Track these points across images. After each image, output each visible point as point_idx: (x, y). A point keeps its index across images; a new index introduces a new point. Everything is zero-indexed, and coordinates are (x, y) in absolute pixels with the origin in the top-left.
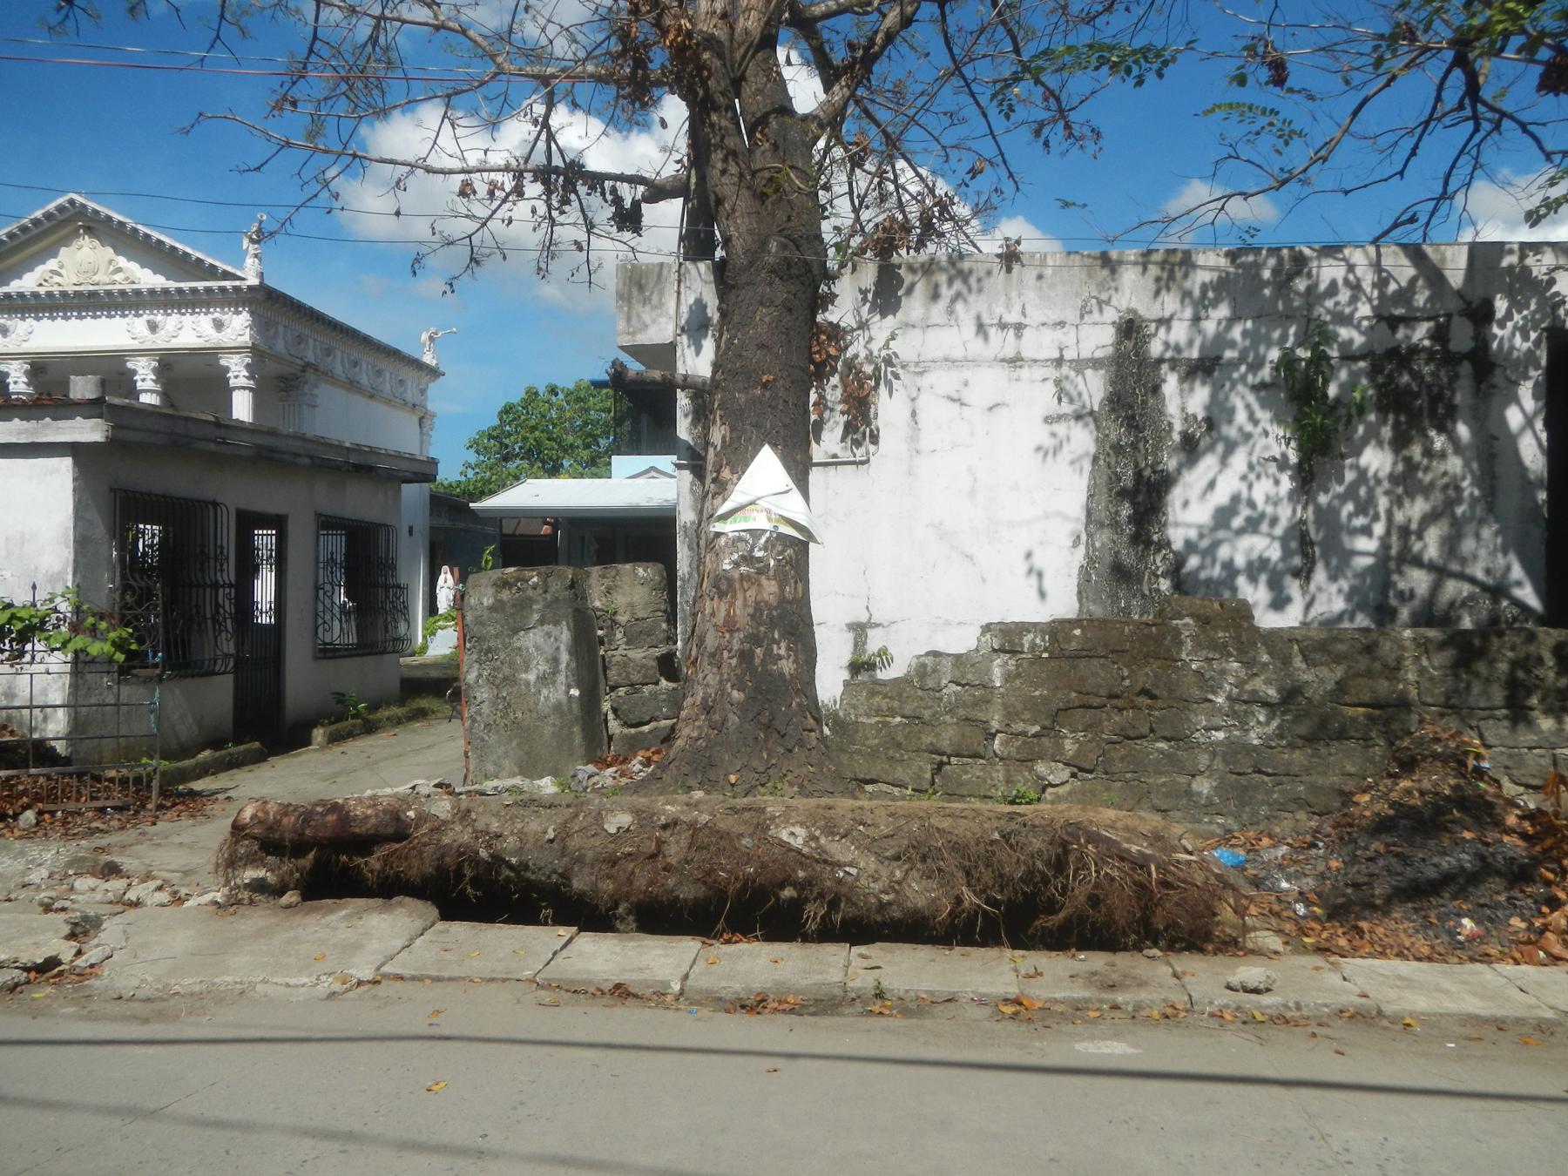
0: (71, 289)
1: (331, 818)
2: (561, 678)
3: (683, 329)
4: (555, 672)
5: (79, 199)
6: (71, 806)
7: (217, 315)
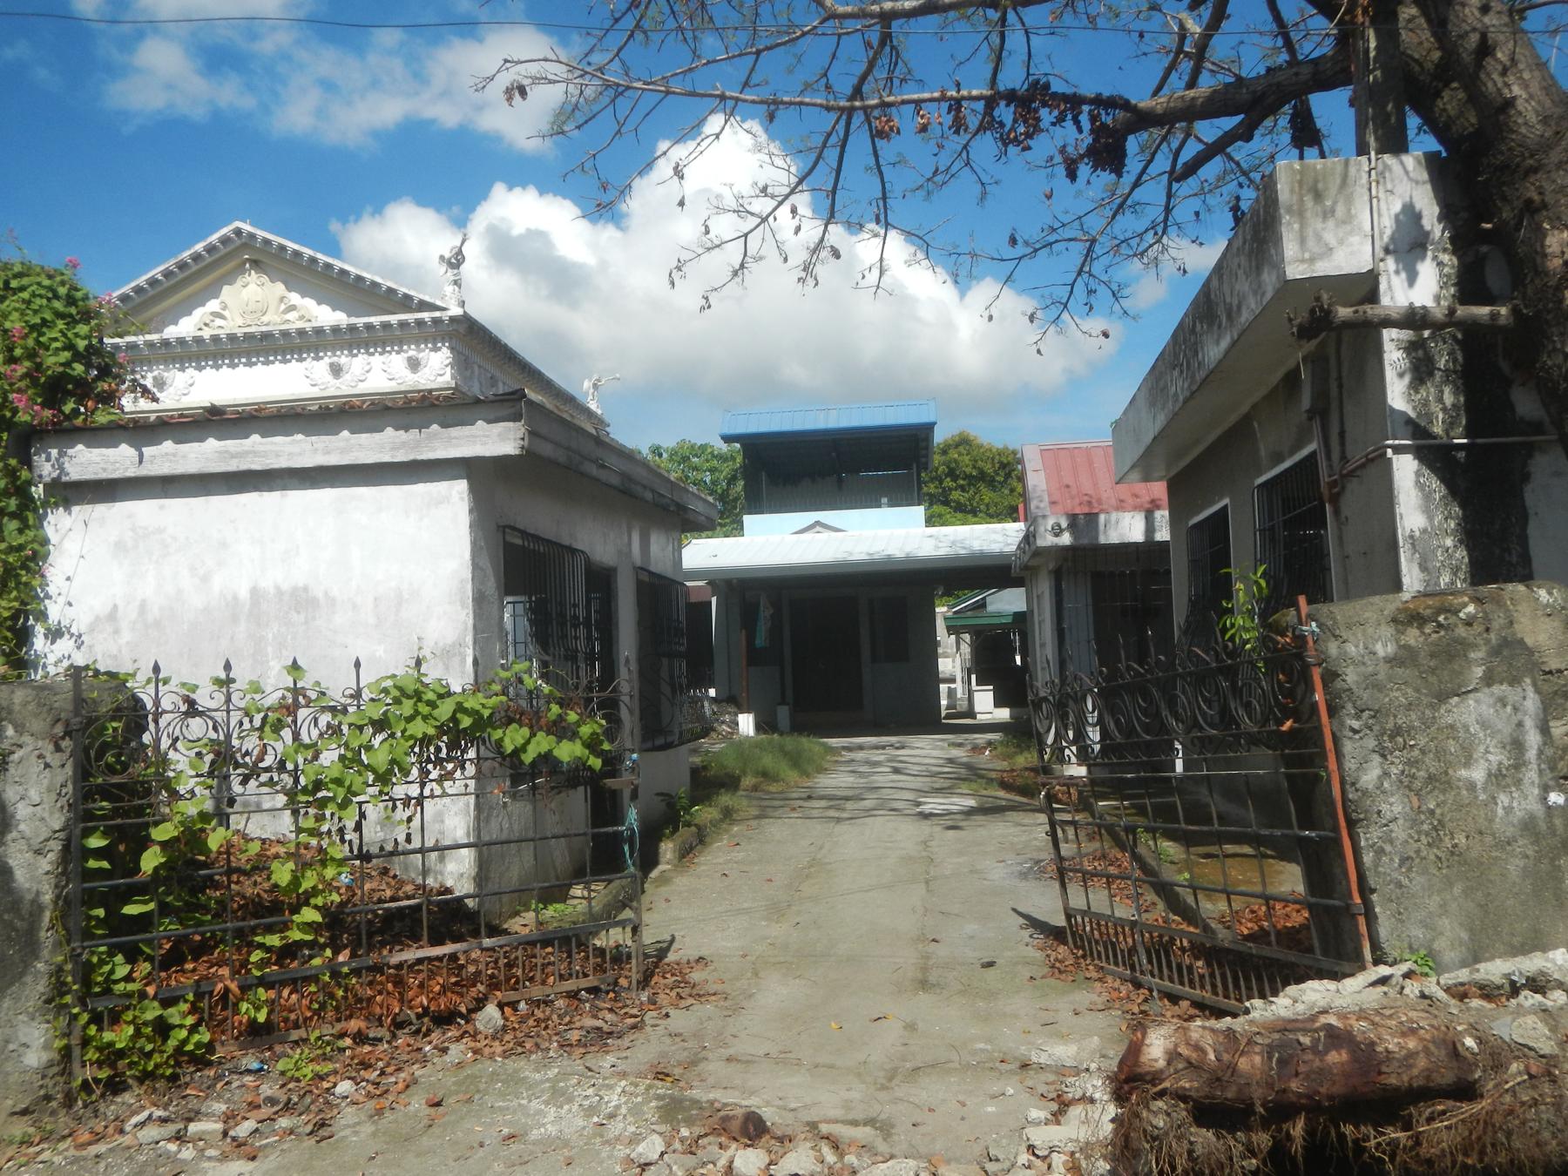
0: (240, 332)
1: (1336, 1057)
2: (1531, 775)
3: (1387, 251)
4: (1519, 764)
5: (247, 227)
6: (537, 992)
7: (411, 353)
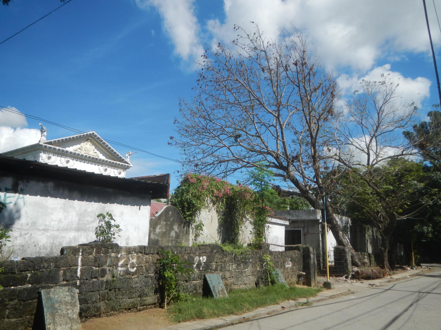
5: (96, 133)
